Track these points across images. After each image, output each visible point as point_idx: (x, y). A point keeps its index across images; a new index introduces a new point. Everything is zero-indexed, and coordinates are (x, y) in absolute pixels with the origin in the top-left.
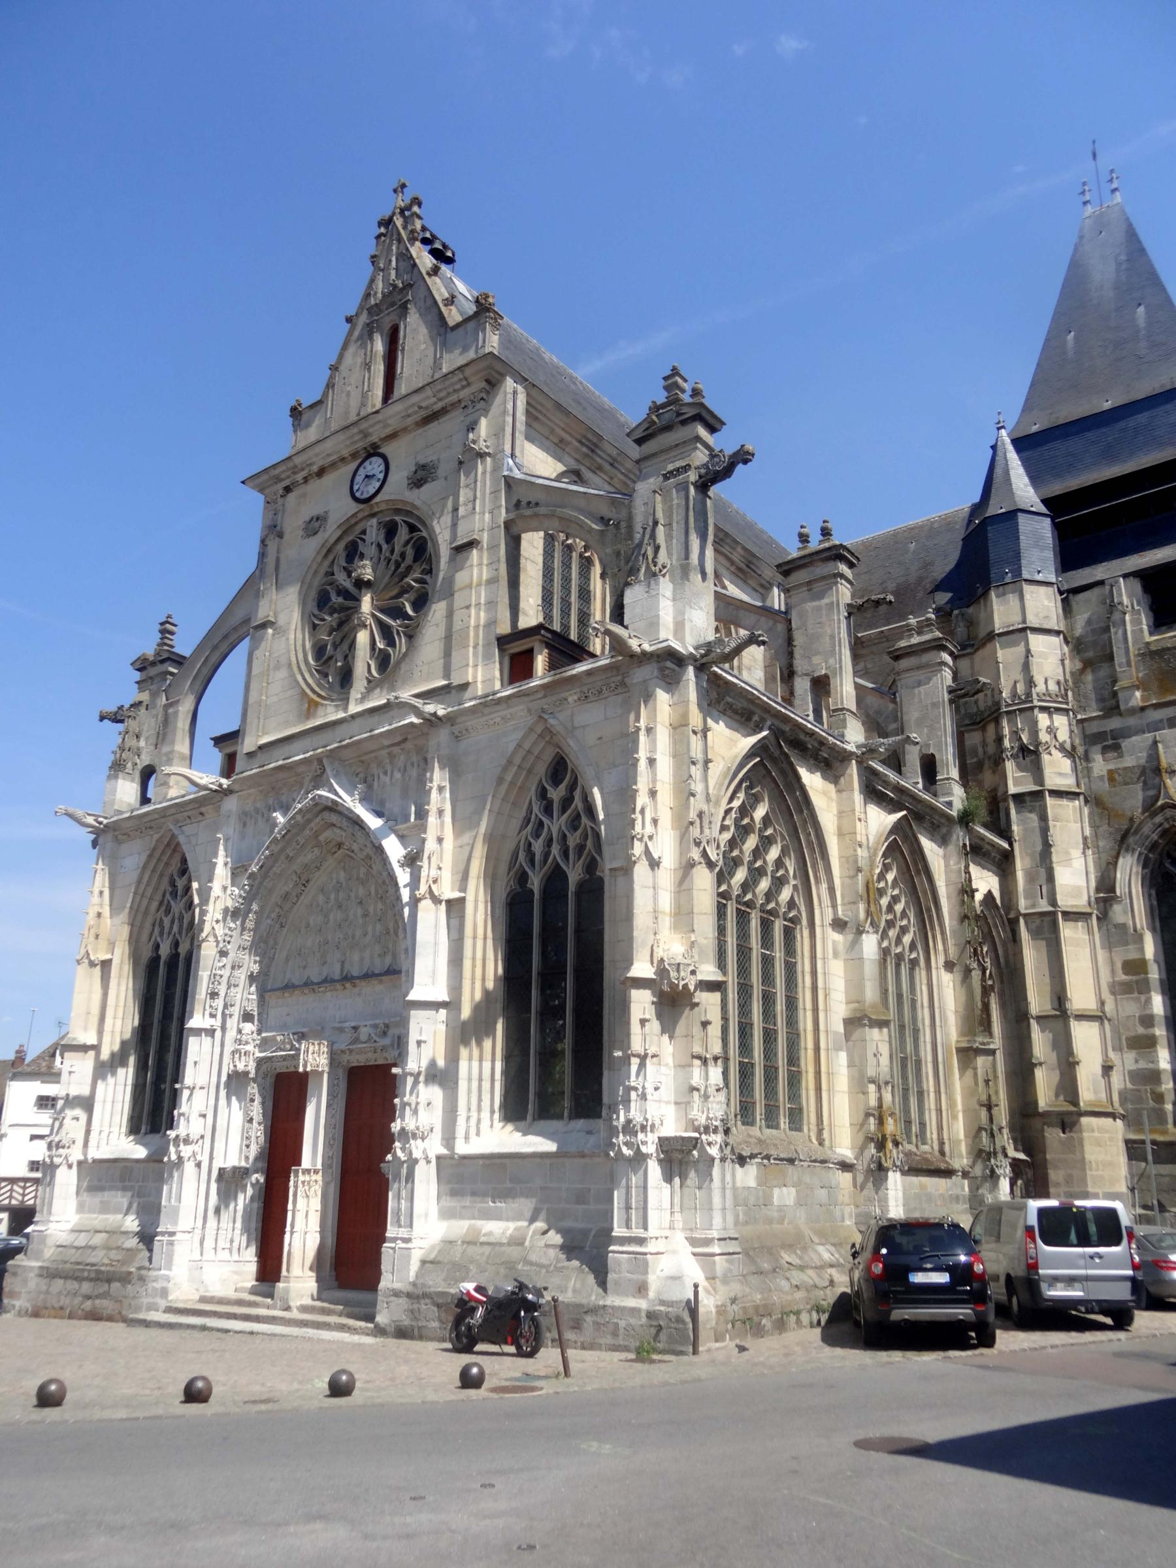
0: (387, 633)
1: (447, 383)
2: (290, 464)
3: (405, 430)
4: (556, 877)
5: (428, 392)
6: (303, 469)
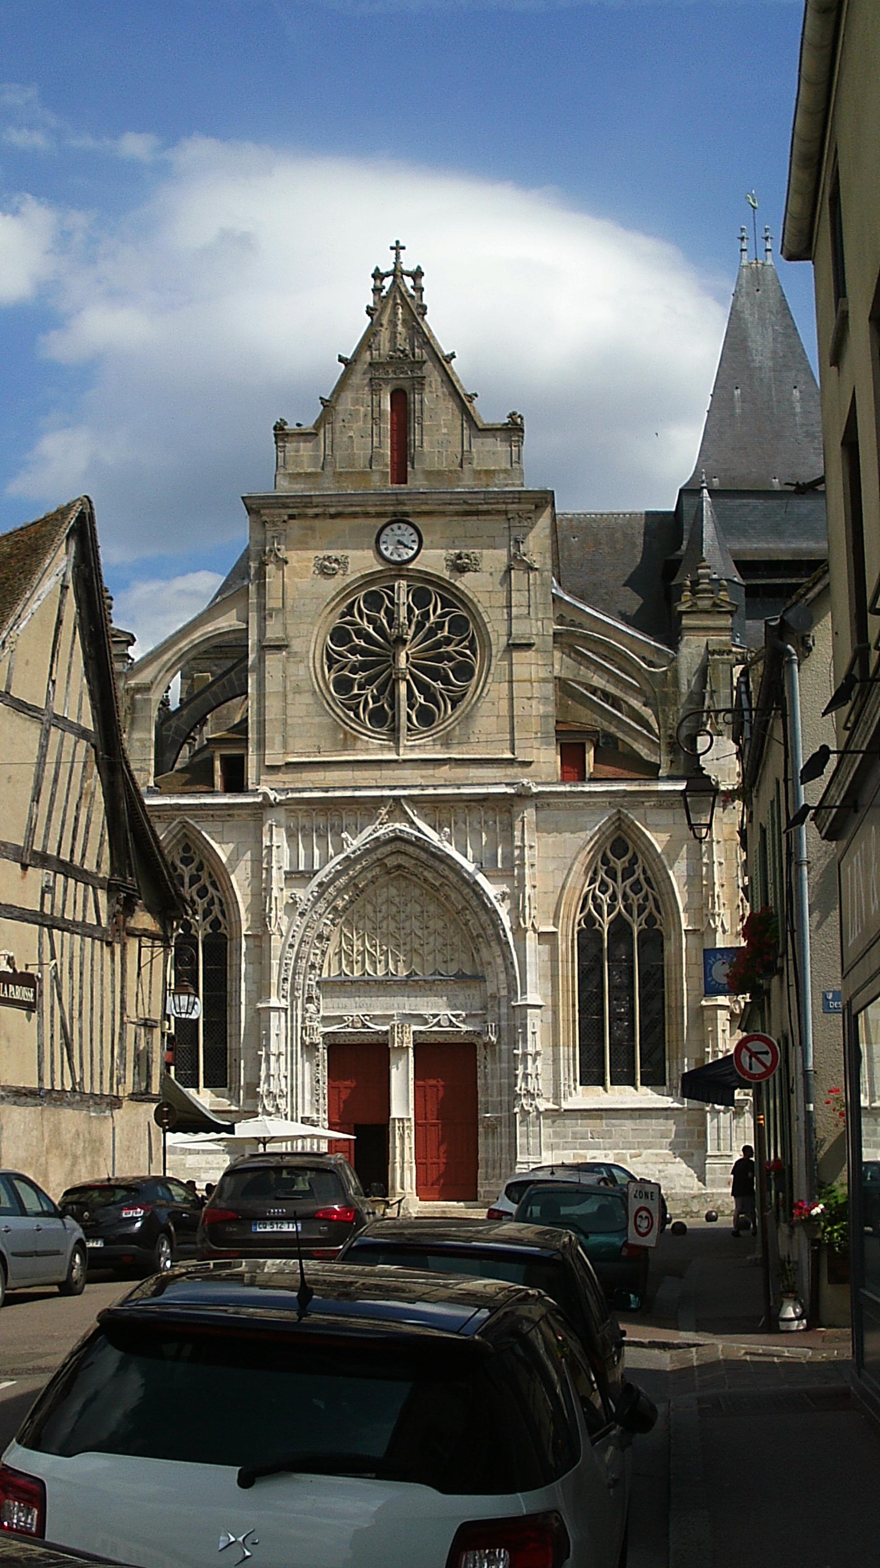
0: (424, 688)
1: (500, 496)
2: (308, 500)
3: (443, 514)
4: (620, 927)
5: (482, 496)
6: (316, 506)
